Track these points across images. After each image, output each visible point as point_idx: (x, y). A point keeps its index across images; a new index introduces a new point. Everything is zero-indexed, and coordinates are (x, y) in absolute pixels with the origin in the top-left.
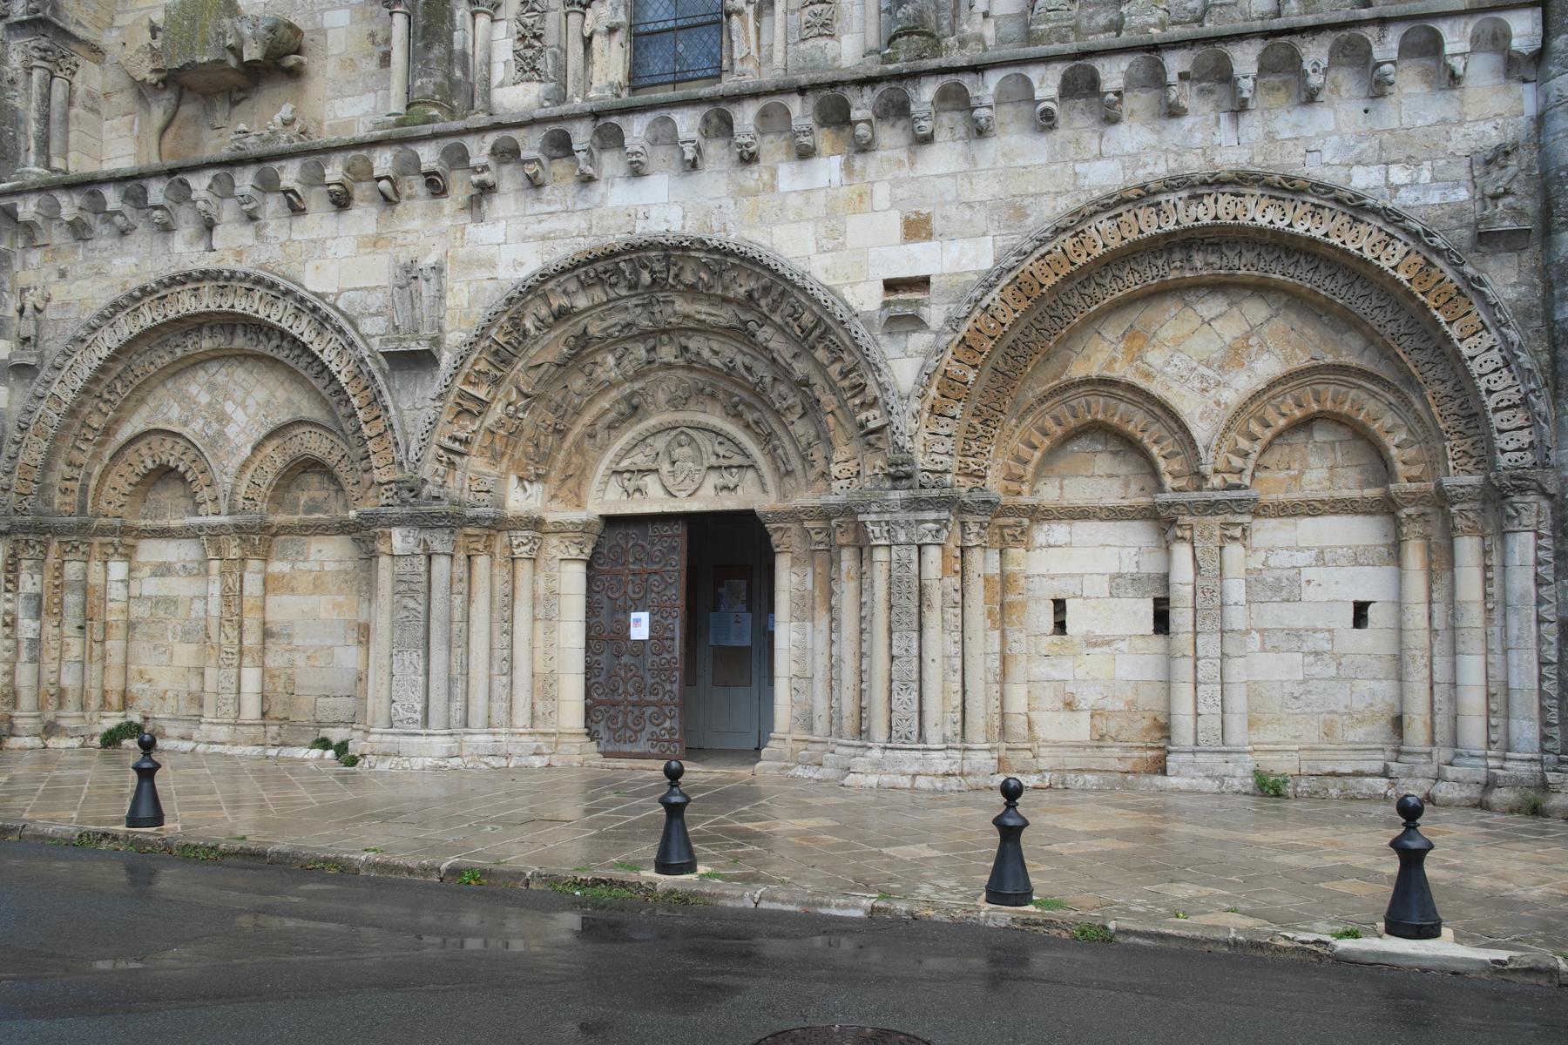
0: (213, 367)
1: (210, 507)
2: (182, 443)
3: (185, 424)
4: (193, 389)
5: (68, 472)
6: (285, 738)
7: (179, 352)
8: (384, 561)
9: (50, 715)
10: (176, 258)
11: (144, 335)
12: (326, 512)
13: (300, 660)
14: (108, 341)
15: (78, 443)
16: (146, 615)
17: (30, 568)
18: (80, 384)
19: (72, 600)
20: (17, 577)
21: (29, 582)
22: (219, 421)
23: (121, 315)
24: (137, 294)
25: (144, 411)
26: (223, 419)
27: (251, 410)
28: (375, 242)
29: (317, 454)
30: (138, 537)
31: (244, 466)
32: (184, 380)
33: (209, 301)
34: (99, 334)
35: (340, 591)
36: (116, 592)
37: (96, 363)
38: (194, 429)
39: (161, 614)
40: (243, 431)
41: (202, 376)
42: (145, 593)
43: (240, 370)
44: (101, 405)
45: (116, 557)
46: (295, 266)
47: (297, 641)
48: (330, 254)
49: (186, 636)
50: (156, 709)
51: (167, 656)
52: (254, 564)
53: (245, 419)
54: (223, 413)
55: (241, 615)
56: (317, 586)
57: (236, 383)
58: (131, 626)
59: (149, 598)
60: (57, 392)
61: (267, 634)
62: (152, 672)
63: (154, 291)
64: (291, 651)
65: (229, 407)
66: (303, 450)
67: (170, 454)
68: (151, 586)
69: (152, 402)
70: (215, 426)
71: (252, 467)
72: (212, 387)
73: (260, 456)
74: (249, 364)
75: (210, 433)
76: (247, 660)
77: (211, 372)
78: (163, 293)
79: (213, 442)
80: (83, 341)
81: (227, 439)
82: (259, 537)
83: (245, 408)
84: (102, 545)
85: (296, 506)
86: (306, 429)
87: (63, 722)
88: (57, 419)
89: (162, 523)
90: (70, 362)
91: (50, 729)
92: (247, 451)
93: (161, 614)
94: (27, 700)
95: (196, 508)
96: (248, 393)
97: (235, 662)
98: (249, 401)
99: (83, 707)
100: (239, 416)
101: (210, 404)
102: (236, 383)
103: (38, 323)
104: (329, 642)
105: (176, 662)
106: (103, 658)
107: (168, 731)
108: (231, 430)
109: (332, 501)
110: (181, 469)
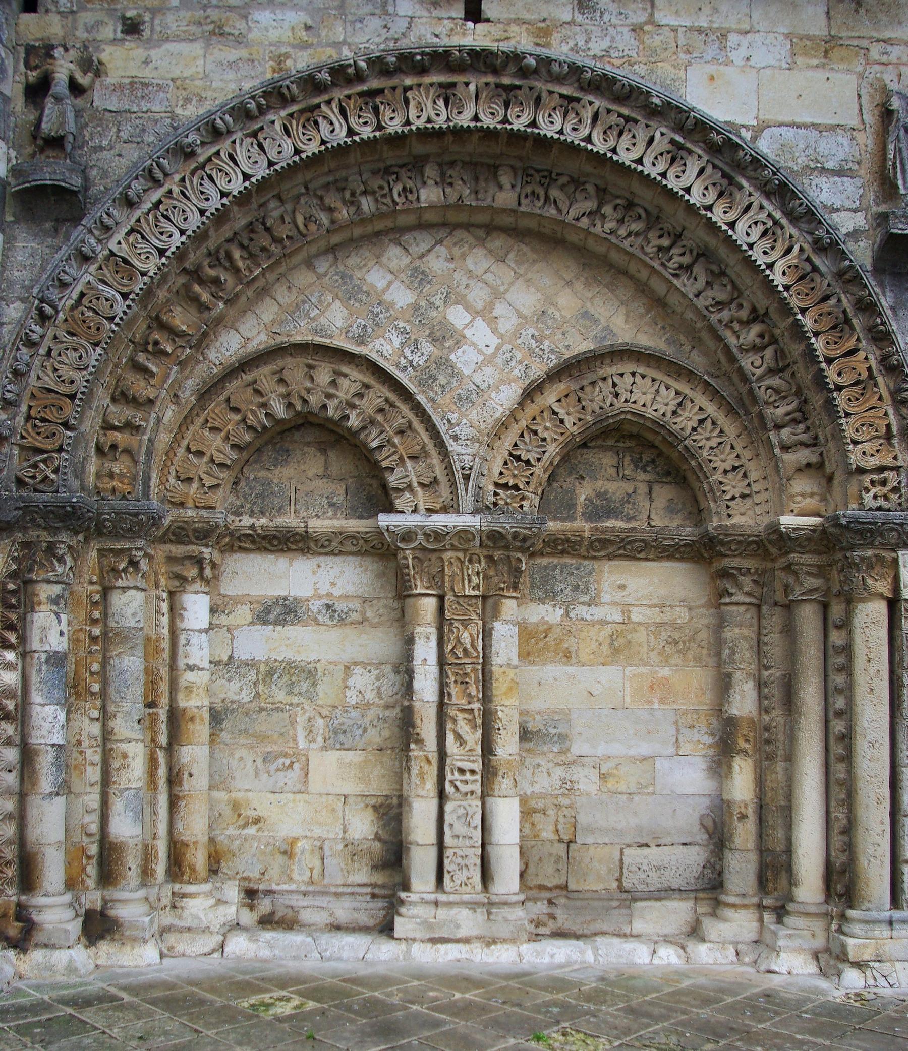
0: (421, 242)
1: (422, 498)
2: (355, 374)
3: (361, 340)
4: (376, 278)
5: (120, 414)
6: (563, 919)
7: (367, 204)
8: (871, 617)
9: (93, 898)
10: (399, 26)
11: (306, 165)
12: (630, 519)
13: (587, 781)
14: (245, 164)
15: (141, 358)
16: (245, 696)
17: (55, 601)
18: (177, 240)
19: (130, 663)
20: (23, 619)
21: (50, 630)
22: (434, 340)
23: (278, 117)
24: (325, 76)
25: (268, 311)
26: (443, 336)
27: (507, 325)
28: (828, 48)
29: (649, 413)
30: (231, 549)
31: (503, 426)
32: (353, 260)
33: (474, 112)
34: (224, 146)
35: (666, 660)
36: (198, 651)
37: (215, 203)
38: (384, 348)
39: (281, 696)
40: (489, 360)
41: (394, 256)
42: (243, 653)
43: (480, 252)
44: (197, 288)
45: (197, 586)
46: (665, 69)
47: (578, 748)
48: (737, 57)
49: (337, 737)
50: (274, 873)
51: (295, 774)
52: (509, 607)
53: (494, 341)
54: (444, 324)
55: (486, 698)
56: (618, 648)
57: (470, 274)
58: (216, 717)
59: (251, 664)
60: (124, 250)
61: (525, 735)
62: (260, 802)
63: (359, 77)
64: (568, 764)
65: (457, 316)
66: (619, 404)
67: (339, 394)
68: (257, 643)
69: (284, 296)
70: (427, 347)
71: (515, 431)
72: (419, 277)
73: (531, 409)
74: (498, 242)
75: (416, 359)
76: (503, 784)
77: (415, 250)
78: (374, 83)
79: (427, 379)
80: (190, 155)
81: (454, 373)
82: (512, 557)
83: (492, 322)
84: (171, 559)
85: (572, 506)
86: (628, 367)
87: (122, 912)
88: (120, 306)
89: (289, 520)
90: (156, 196)
91: (98, 926)
92: (507, 396)
93: (281, 696)
94: (53, 871)
95: (382, 499)
96: (497, 295)
97: (477, 788)
98: (500, 309)
99: (146, 872)
100: (481, 334)
101: (416, 307)
102: (470, 274)
103: (78, 113)
104: (644, 749)
105: (315, 783)
106: (174, 780)
107: (306, 916)
108: (464, 359)
109: (642, 501)
110: (354, 422)
